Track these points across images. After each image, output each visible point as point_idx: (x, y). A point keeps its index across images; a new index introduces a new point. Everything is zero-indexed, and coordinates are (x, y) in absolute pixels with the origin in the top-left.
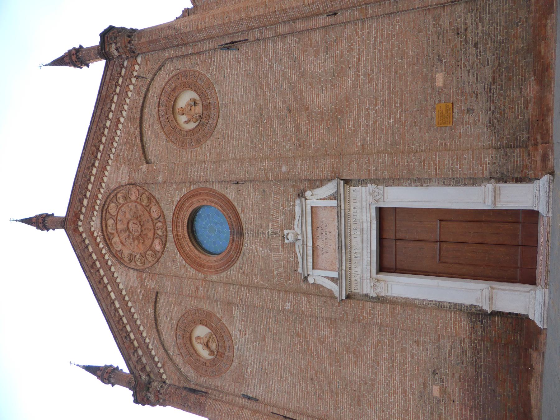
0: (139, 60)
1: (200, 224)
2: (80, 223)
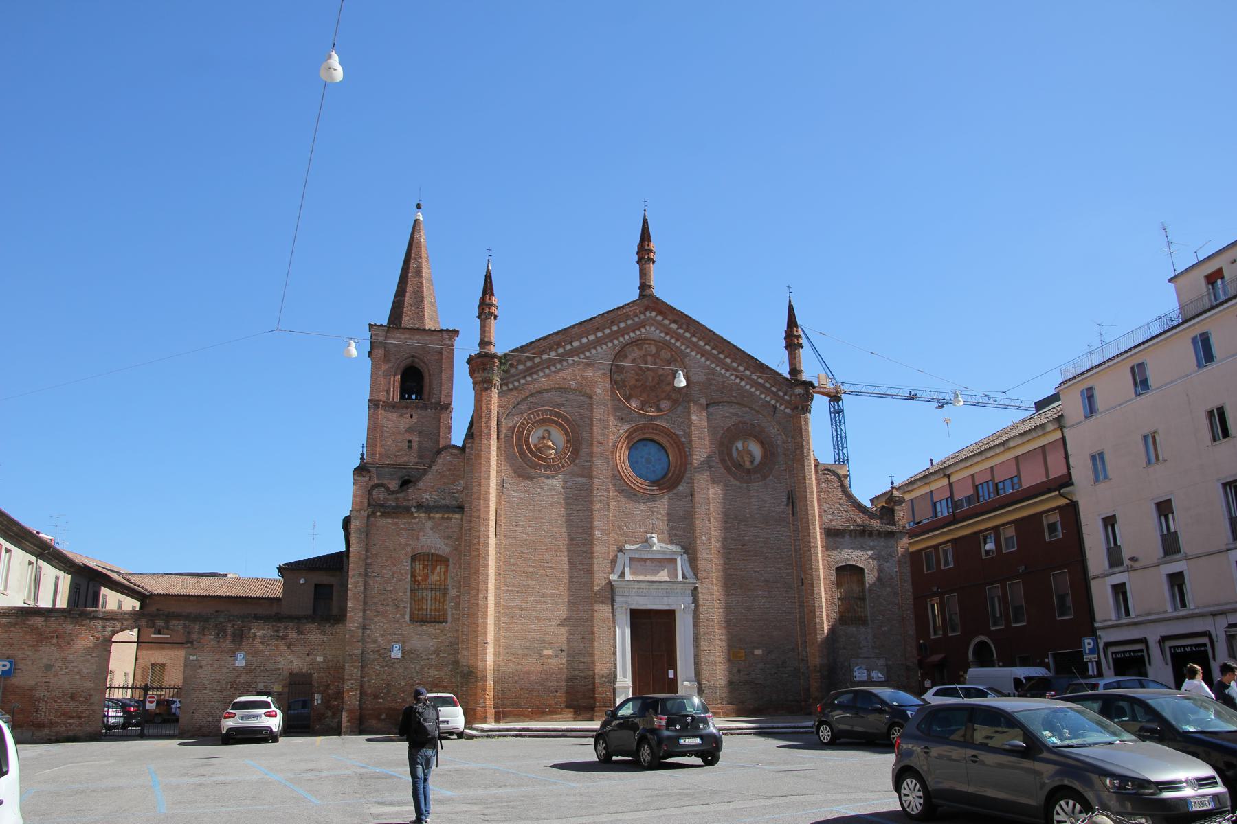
0: (788, 411)
1: (651, 445)
2: (654, 314)
